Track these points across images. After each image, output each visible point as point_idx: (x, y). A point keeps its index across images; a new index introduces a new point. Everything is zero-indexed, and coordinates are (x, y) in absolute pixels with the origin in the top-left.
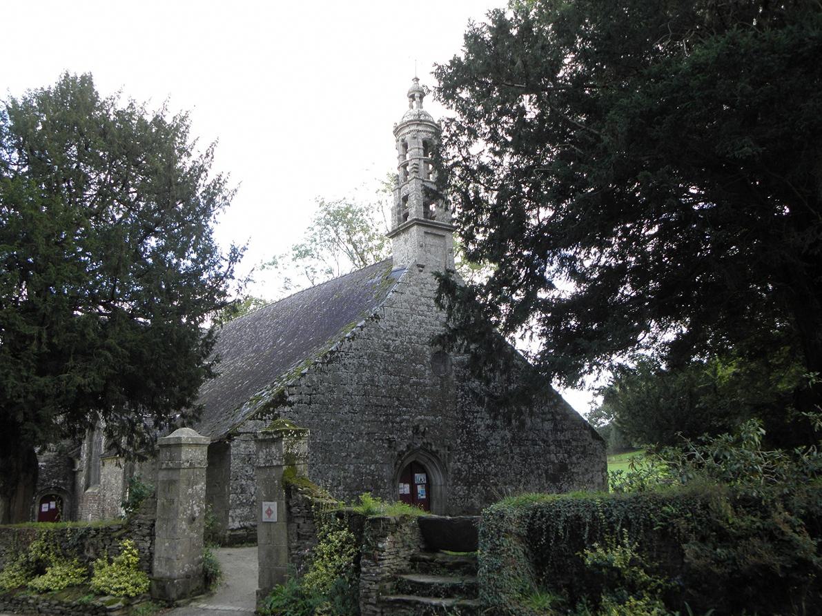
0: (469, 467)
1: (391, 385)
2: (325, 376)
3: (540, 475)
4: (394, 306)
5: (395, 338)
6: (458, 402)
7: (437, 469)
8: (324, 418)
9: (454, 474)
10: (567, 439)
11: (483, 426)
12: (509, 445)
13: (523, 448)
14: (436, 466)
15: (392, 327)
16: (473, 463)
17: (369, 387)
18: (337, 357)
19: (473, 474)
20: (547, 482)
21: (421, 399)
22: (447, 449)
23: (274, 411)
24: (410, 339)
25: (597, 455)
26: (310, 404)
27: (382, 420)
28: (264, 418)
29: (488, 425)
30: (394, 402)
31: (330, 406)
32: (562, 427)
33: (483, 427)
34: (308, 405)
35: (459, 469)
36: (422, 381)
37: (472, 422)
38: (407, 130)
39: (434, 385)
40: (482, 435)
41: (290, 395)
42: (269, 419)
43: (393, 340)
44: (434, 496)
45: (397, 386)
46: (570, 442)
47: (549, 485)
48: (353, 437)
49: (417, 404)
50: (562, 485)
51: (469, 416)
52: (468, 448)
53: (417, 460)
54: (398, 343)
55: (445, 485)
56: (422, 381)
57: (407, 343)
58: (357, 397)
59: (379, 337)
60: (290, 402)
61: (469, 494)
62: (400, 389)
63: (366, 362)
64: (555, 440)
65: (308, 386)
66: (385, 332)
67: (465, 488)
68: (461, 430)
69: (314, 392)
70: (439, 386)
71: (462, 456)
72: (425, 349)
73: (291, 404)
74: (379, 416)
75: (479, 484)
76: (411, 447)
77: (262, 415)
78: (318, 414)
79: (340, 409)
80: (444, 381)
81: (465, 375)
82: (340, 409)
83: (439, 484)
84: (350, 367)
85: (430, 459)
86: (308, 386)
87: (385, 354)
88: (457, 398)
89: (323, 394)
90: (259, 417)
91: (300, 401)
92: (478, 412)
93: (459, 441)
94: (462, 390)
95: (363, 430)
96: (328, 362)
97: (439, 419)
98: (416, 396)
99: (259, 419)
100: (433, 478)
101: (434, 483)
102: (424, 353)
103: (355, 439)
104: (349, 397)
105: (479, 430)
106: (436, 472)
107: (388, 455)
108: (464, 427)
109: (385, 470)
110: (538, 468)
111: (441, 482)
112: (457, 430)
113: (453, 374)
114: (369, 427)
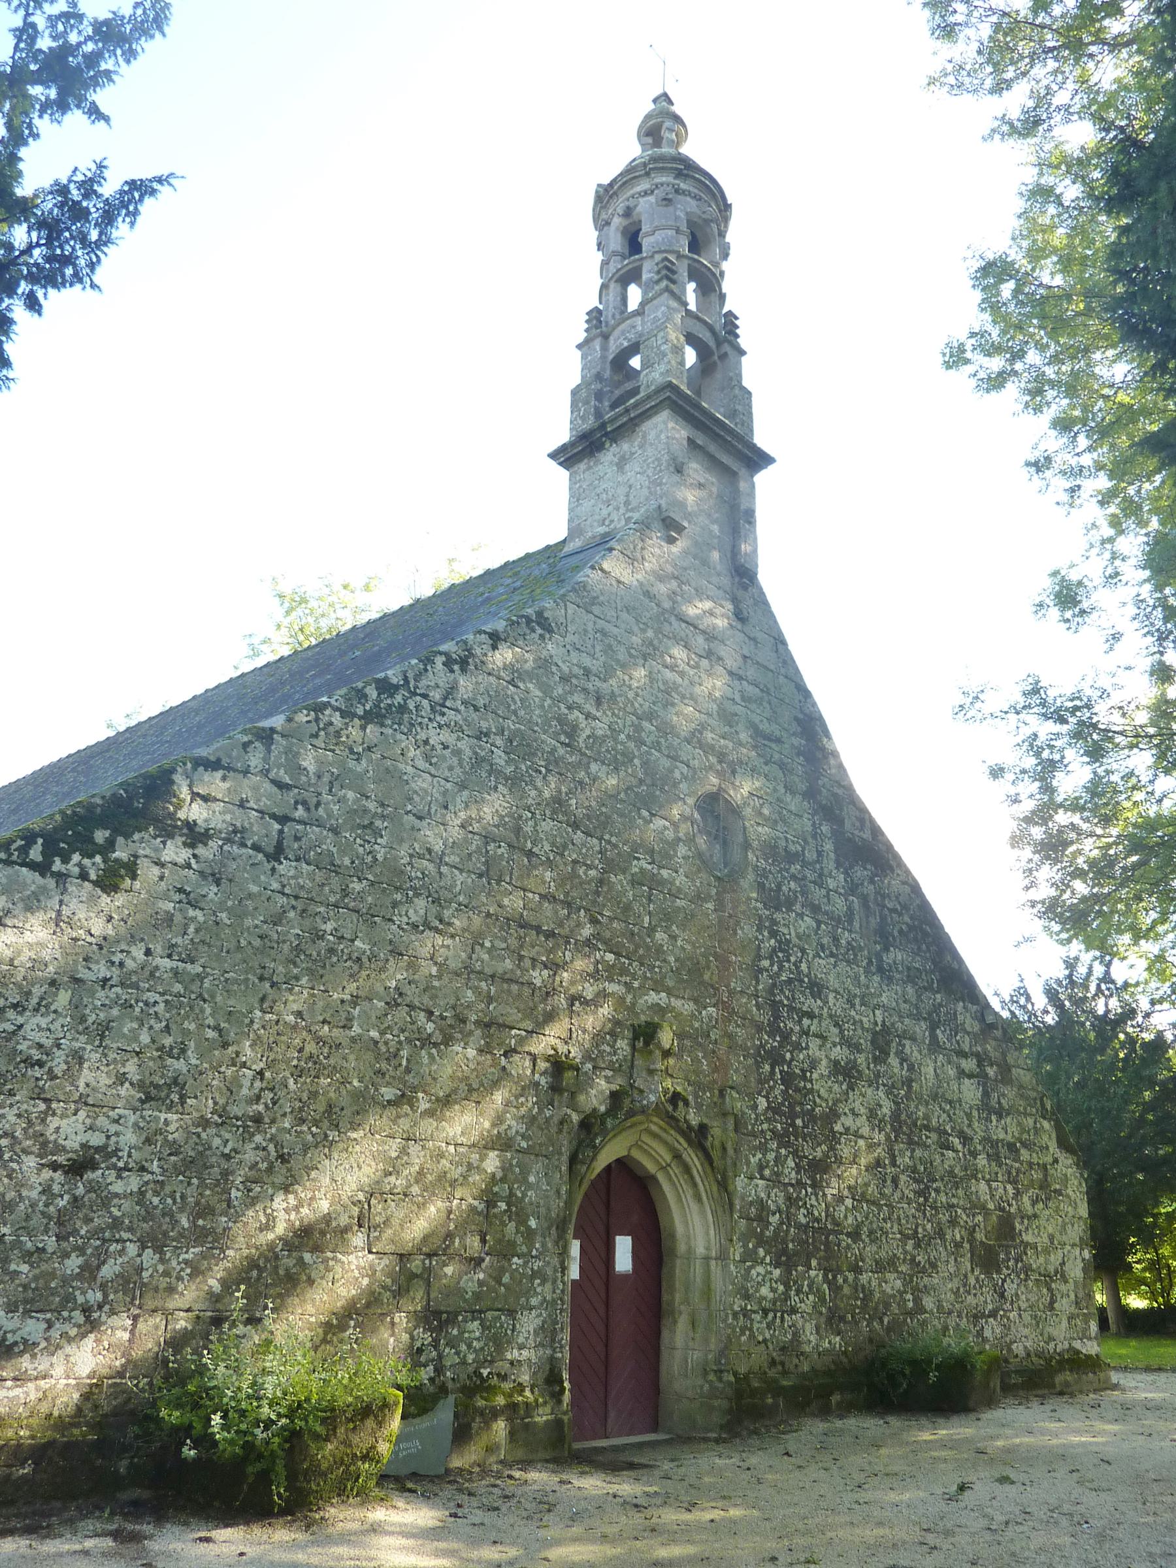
0: (789, 1198)
1: (575, 862)
2: (351, 764)
3: (958, 1245)
4: (596, 610)
5: (594, 711)
6: (761, 971)
7: (699, 1199)
8: (329, 927)
9: (749, 1219)
10: (1009, 1138)
11: (824, 1062)
12: (888, 1138)
13: (918, 1153)
14: (695, 1185)
15: (587, 672)
16: (800, 1184)
17: (503, 850)
18: (403, 709)
19: (799, 1226)
20: (973, 1270)
21: (660, 936)
22: (731, 1125)
23: (110, 844)
24: (638, 729)
25: (1068, 1196)
26: (277, 853)
27: (538, 982)
28: (57, 865)
29: (836, 1063)
30: (579, 925)
31: (356, 886)
32: (999, 1103)
33: (823, 1068)
34: (268, 857)
35: (762, 1205)
36: (665, 873)
37: (798, 1047)
38: (644, 185)
39: (699, 898)
40: (822, 1092)
41: (195, 795)
42: (84, 876)
43: (588, 716)
44: (678, 1297)
45: (593, 873)
46: (1017, 1151)
47: (977, 1279)
48: (430, 1027)
49: (648, 948)
50: (1004, 1281)
51: (790, 1025)
52: (786, 1133)
53: (636, 1154)
54: (601, 728)
55: (723, 1257)
56: (665, 873)
57: (628, 736)
58: (460, 878)
59: (546, 690)
60: (190, 826)
61: (787, 1297)
62: (601, 882)
63: (500, 758)
64: (986, 1140)
65: (280, 785)
66: (564, 679)
67: (777, 1273)
68: (767, 1067)
69: (300, 812)
70: (710, 906)
71: (771, 1156)
72: (677, 774)
73: (195, 835)
74: (527, 963)
75: (814, 1263)
76: (627, 1102)
77: (50, 851)
78: (305, 903)
79: (395, 904)
80: (724, 891)
81: (779, 886)
82: (395, 904)
83: (700, 1250)
84: (444, 758)
85: (677, 1156)
86: (280, 785)
87: (561, 751)
88: (759, 957)
89: (335, 831)
90: (35, 853)
91: (236, 835)
92: (811, 1015)
93: (762, 1103)
94: (773, 934)
95: (469, 1006)
96: (368, 718)
97: (710, 1017)
98: (647, 919)
99: (33, 866)
100: (680, 1229)
101: (682, 1248)
102: (675, 785)
103: (436, 1037)
104: (431, 867)
105: (815, 1076)
106: (694, 1206)
107: (547, 1120)
108: (776, 1059)
109: (532, 1179)
110: (953, 1222)
111: (708, 1249)
112: (758, 1065)
113: (751, 877)
114: (490, 999)
